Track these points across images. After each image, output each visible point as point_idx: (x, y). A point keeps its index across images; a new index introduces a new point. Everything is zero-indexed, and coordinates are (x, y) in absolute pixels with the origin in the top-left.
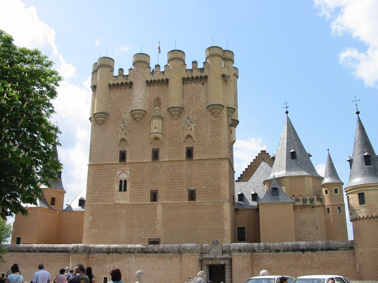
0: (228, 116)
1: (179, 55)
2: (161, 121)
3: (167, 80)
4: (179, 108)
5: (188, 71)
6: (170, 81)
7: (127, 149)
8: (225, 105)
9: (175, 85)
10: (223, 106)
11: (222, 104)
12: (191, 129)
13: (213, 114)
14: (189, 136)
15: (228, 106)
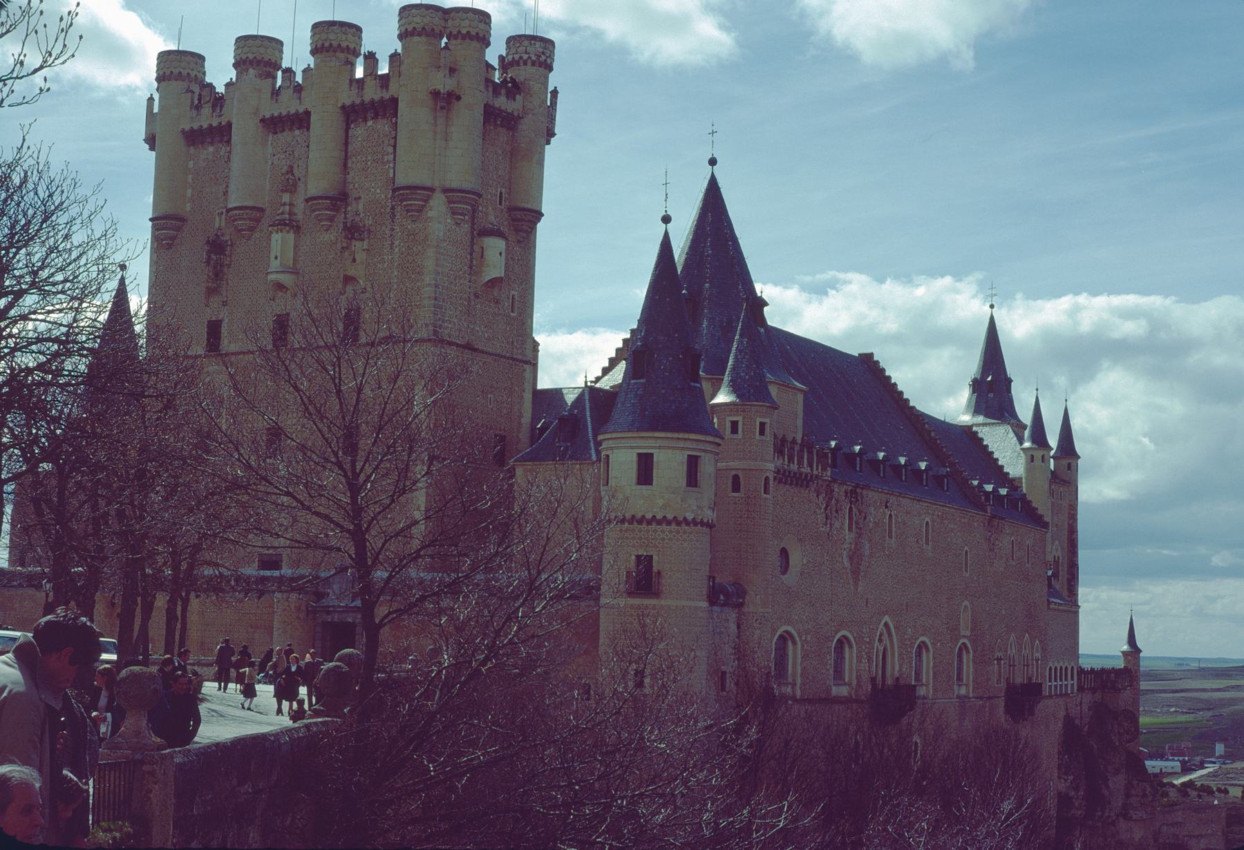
0: (454, 213)
1: (332, 36)
2: (291, 236)
3: (308, 113)
4: (326, 198)
5: (354, 84)
6: (313, 118)
7: (223, 314)
8: (437, 184)
9: (324, 127)
10: (432, 190)
11: (428, 183)
12: (354, 260)
13: (408, 211)
14: (348, 279)
15: (447, 186)
